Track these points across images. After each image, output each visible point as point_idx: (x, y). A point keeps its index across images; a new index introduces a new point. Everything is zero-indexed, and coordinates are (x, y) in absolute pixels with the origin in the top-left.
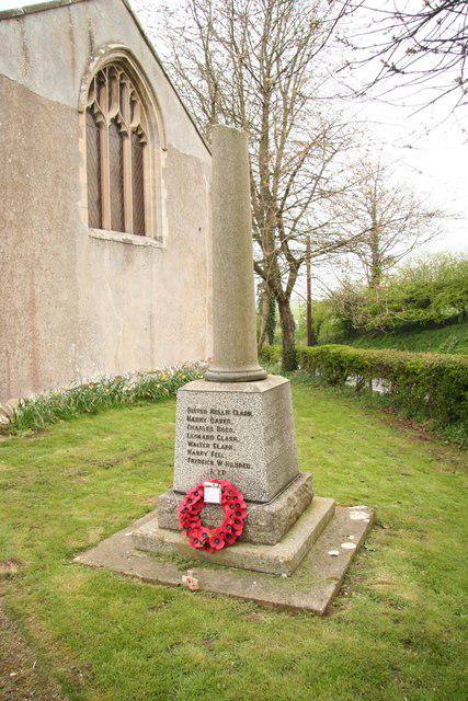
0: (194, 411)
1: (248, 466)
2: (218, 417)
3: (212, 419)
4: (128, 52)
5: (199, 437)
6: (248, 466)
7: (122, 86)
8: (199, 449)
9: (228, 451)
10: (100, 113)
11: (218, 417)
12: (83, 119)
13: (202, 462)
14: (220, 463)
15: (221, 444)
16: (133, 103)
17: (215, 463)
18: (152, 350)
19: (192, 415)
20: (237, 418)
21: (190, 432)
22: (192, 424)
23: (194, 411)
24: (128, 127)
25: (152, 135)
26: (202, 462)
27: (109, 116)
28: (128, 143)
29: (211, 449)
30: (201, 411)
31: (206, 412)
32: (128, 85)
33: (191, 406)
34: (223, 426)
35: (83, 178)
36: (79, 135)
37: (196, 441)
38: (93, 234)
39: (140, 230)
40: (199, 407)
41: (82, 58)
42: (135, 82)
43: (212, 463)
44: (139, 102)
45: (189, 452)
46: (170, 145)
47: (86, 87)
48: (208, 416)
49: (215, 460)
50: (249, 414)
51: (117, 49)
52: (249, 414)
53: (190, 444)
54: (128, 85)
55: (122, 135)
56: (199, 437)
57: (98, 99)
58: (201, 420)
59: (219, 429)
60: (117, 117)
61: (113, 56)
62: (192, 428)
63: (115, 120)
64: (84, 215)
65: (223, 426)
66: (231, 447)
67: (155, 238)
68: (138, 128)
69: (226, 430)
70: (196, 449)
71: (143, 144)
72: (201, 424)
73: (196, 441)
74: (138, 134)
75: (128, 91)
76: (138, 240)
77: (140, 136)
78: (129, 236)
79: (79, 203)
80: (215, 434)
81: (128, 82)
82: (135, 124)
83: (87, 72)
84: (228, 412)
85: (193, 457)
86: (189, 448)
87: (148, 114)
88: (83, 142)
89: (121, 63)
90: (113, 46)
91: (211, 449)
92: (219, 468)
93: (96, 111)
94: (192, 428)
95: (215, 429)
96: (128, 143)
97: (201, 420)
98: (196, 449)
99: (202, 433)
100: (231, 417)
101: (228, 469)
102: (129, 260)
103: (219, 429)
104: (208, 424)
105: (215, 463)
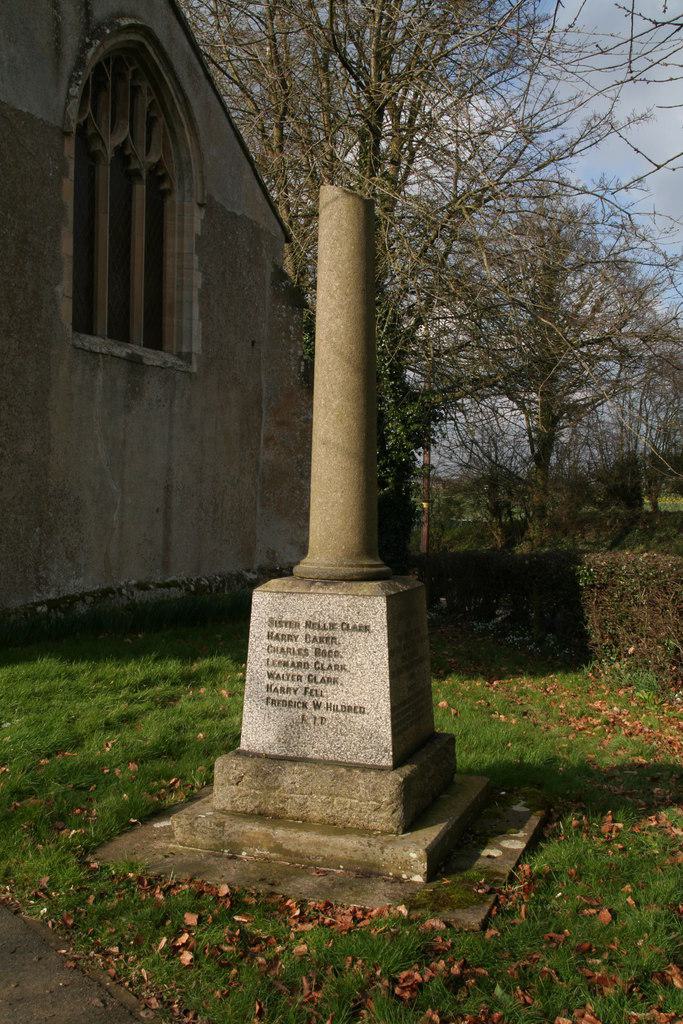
0: (280, 623)
1: (362, 710)
2: (317, 633)
3: (307, 636)
4: (148, 33)
5: (286, 664)
6: (362, 710)
7: (135, 90)
8: (285, 684)
9: (330, 687)
10: (98, 135)
11: (317, 633)
12: (70, 148)
13: (289, 704)
14: (317, 706)
15: (321, 675)
16: (151, 122)
17: (310, 705)
18: (167, 547)
19: (276, 631)
20: (347, 635)
21: (272, 656)
22: (275, 644)
23: (280, 623)
24: (143, 161)
25: (181, 179)
26: (289, 704)
27: (113, 142)
28: (140, 191)
29: (305, 683)
30: (289, 624)
31: (297, 625)
32: (145, 91)
33: (274, 615)
34: (324, 647)
35: (67, 246)
36: (64, 173)
37: (280, 671)
38: (78, 343)
39: (155, 340)
40: (287, 617)
41: (71, 42)
42: (158, 86)
43: (305, 705)
44: (162, 120)
45: (269, 688)
46: (210, 198)
47: (76, 91)
48: (301, 632)
49: (309, 701)
50: (366, 629)
51: (131, 27)
52: (366, 629)
53: (270, 676)
54: (145, 91)
56: (286, 664)
58: (290, 637)
60: (124, 143)
61: (122, 38)
62: (275, 650)
63: (120, 150)
64: (66, 309)
65: (324, 647)
66: (335, 681)
67: (179, 355)
68: (159, 165)
70: (280, 684)
71: (165, 194)
72: (290, 644)
73: (280, 671)
74: (157, 178)
75: (145, 101)
76: (152, 357)
77: (162, 179)
78: (139, 350)
79: (59, 289)
80: (311, 659)
81: (145, 85)
82: (154, 159)
83: (80, 63)
84: (333, 626)
85: (274, 696)
86: (269, 681)
87: (175, 141)
88: (68, 185)
89: (135, 52)
90: (125, 22)
91: (305, 683)
92: (317, 713)
93: (90, 131)
94: (275, 650)
95: (311, 653)
96: (140, 191)
97: (290, 637)
98: (280, 684)
99: (290, 658)
100: (338, 633)
101: (329, 715)
102: (134, 392)
103: (317, 652)
104: (301, 644)
105: (310, 705)
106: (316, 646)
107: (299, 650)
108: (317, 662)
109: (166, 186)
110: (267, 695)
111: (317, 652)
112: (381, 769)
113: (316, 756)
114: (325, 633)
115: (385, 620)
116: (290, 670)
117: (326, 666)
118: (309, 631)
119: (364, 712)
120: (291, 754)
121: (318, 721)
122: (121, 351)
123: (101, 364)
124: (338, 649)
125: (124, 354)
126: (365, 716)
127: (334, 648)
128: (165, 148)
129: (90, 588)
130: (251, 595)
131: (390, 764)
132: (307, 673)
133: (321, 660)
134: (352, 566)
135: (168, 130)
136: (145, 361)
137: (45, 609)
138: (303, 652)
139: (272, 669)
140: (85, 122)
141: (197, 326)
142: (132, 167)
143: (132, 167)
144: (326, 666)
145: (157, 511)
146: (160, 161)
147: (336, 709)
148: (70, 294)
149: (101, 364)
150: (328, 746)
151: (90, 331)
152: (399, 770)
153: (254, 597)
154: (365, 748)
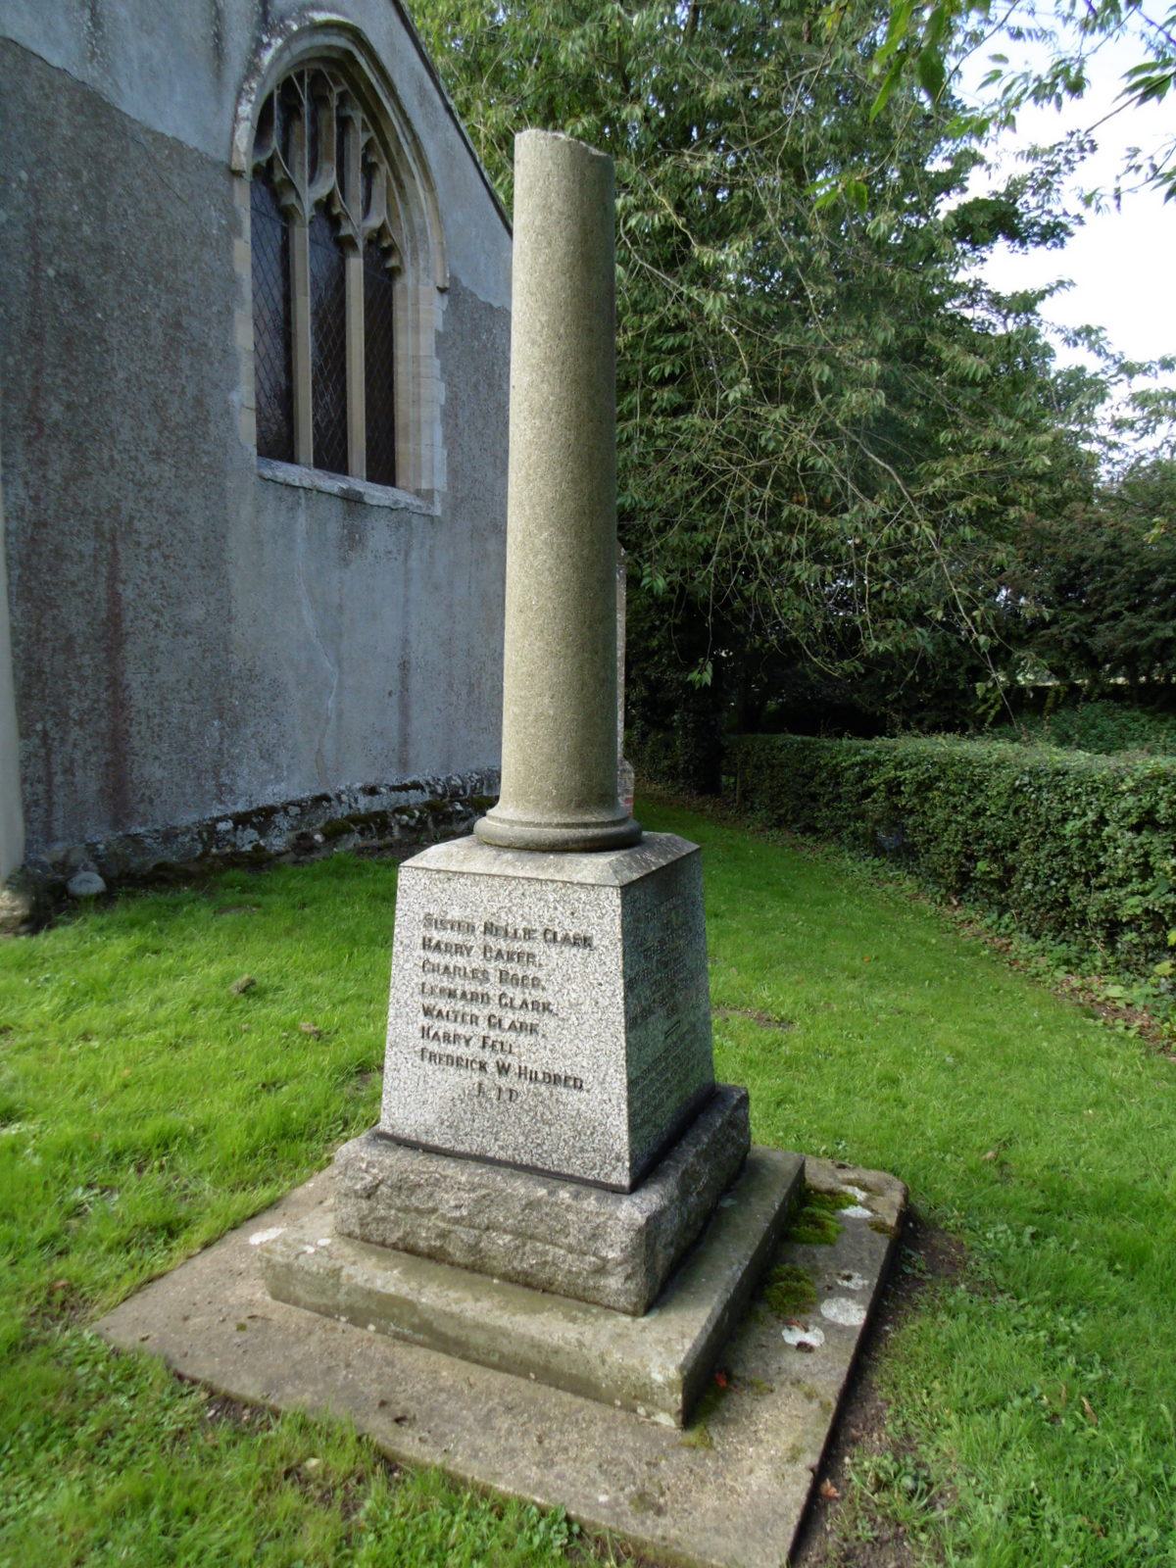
0: (441, 924)
1: (578, 1085)
2: (503, 945)
3: (486, 949)
4: (355, 34)
5: (452, 994)
6: (578, 1085)
7: (344, 123)
8: (451, 1027)
9: (525, 1040)
10: (290, 184)
11: (503, 945)
12: (242, 197)
13: (457, 1062)
14: (503, 1070)
15: (509, 1017)
16: (369, 170)
17: (491, 1068)
18: (405, 741)
19: (436, 936)
20: (554, 951)
21: (431, 979)
22: (435, 958)
23: (441, 924)
24: (359, 225)
25: (415, 251)
26: (457, 1062)
27: (310, 194)
28: (356, 266)
30: (457, 926)
31: (471, 928)
32: (358, 124)
33: (435, 910)
34: (515, 968)
35: (244, 336)
36: (233, 229)
37: (443, 1005)
38: (268, 473)
39: (383, 469)
40: (455, 914)
41: (238, 39)
42: (375, 117)
43: (483, 1067)
44: (384, 167)
46: (454, 279)
47: (247, 109)
48: (476, 940)
49: (491, 1059)
50: (586, 942)
51: (328, 26)
52: (586, 942)
53: (427, 1012)
54: (358, 124)
55: (345, 245)
56: (452, 994)
57: (285, 148)
58: (459, 949)
59: (503, 977)
60: (331, 196)
61: (322, 40)
62: (435, 969)
63: (325, 206)
64: (247, 427)
65: (515, 968)
66: (533, 1029)
67: (418, 493)
68: (382, 232)
69: (520, 982)
70: (442, 1027)
71: (393, 273)
72: (459, 961)
73: (443, 1005)
74: (382, 254)
75: (359, 138)
76: (376, 494)
77: (389, 252)
78: (358, 483)
79: (235, 397)
80: (493, 989)
81: (358, 116)
82: (375, 222)
83: (252, 69)
84: (529, 934)
85: (434, 1047)
87: (405, 202)
88: (242, 250)
89: (343, 63)
90: (320, 17)
91: (482, 1029)
92: (504, 1082)
93: (278, 176)
94: (435, 969)
95: (494, 977)
96: (356, 266)
97: (459, 949)
98: (442, 1027)
99: (459, 984)
100: (537, 947)
101: (523, 1086)
102: (353, 540)
103: (503, 977)
104: (476, 961)
105: (491, 1068)
106: (501, 966)
108: (503, 995)
109: (393, 262)
110: (421, 1043)
113: (502, 1155)
114: (516, 946)
115: (618, 930)
116: (459, 1005)
117: (518, 1002)
118: (491, 940)
120: (460, 1148)
121: (505, 1096)
122: (334, 484)
123: (303, 501)
124: (540, 975)
125: (335, 490)
126: (584, 1094)
127: (532, 971)
128: (390, 208)
129: (297, 794)
131: (626, 1182)
132: (486, 1012)
135: (394, 184)
136: (366, 499)
137: (229, 825)
139: (430, 1001)
140: (270, 162)
141: (440, 454)
142: (343, 233)
143: (343, 233)
145: (390, 694)
146: (383, 226)
147: (534, 1079)
148: (253, 404)
149: (303, 501)
150: (521, 1139)
151: (290, 457)
154: (582, 1150)
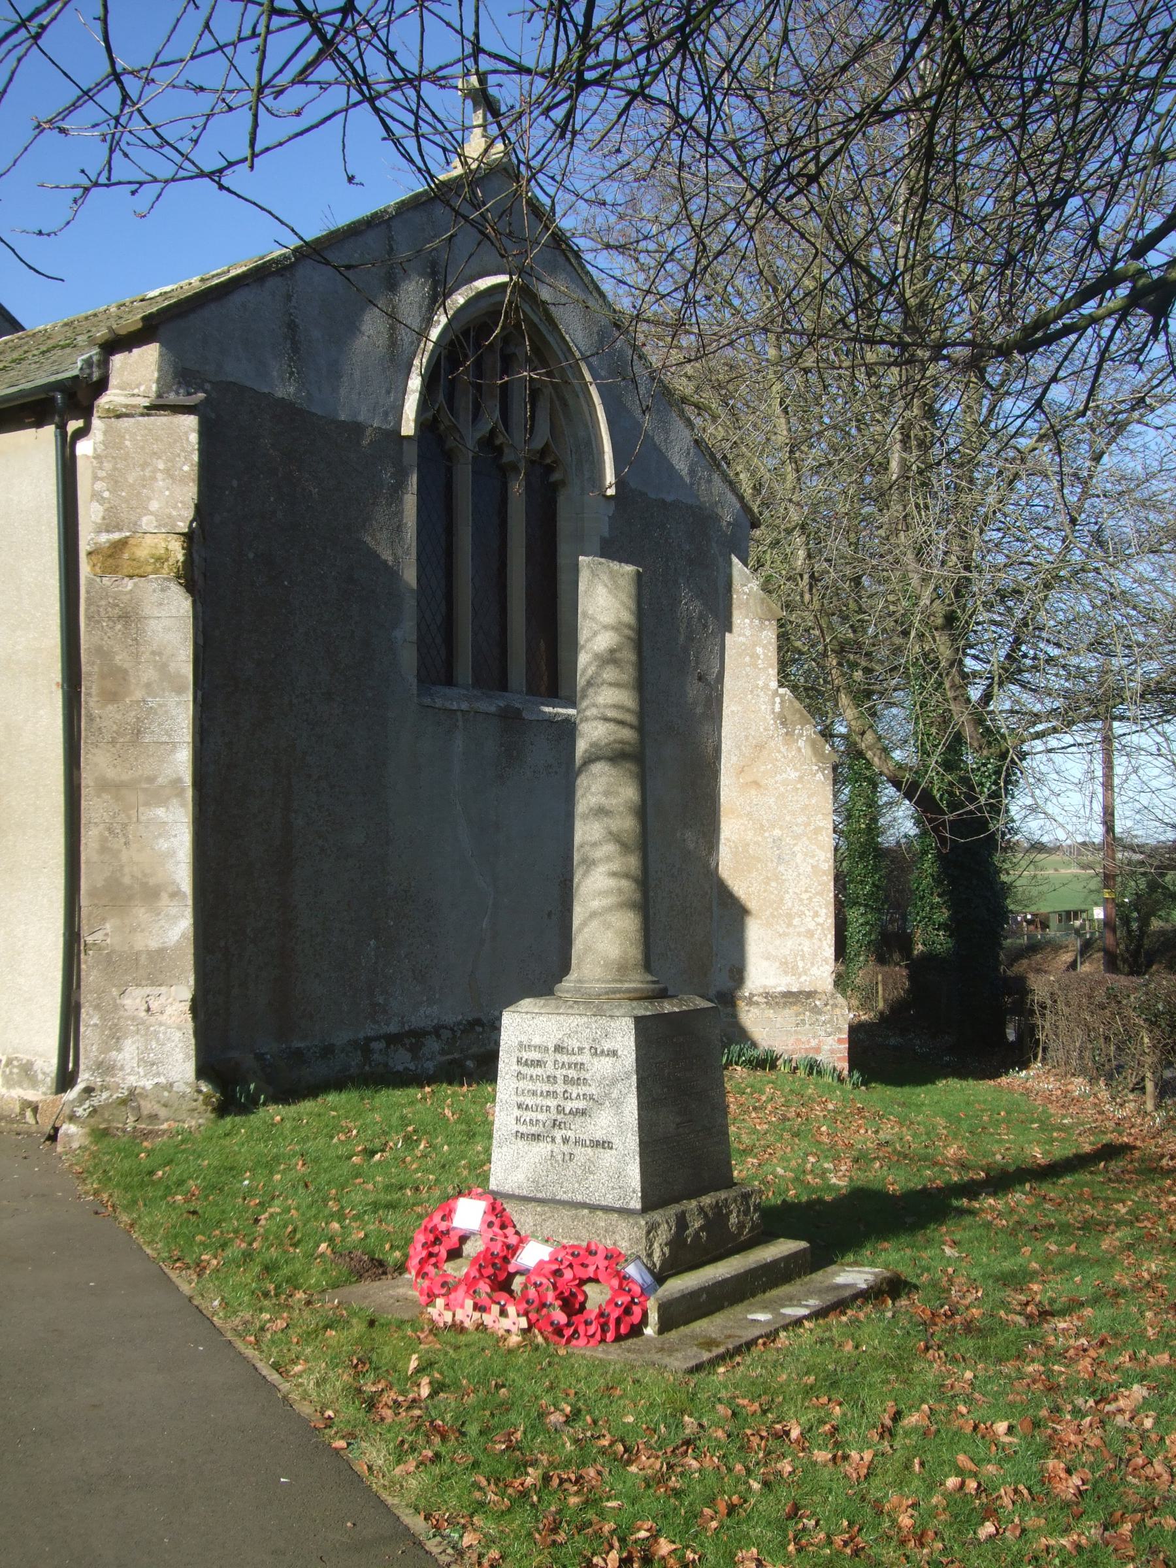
5: (534, 1093)
19: (525, 1055)
20: (596, 1060)
21: (522, 1084)
29: (553, 1115)
31: (547, 1049)
33: (524, 1039)
40: (536, 1040)
45: (518, 1120)
50: (614, 1053)
52: (614, 1053)
53: (519, 1106)
56: (534, 1093)
58: (538, 1063)
59: (566, 1080)
65: (572, 1073)
69: (577, 1082)
72: (539, 1071)
73: (529, 1101)
84: (581, 1049)
92: (565, 1149)
95: (560, 1080)
97: (538, 1063)
98: (528, 1116)
101: (578, 1150)
104: (550, 1069)
105: (559, 1140)
106: (564, 1072)
107: (548, 1077)
108: (566, 1091)
110: (515, 1128)
111: (566, 1080)
112: (624, 1212)
113: (565, 1197)
114: (573, 1059)
115: (633, 1044)
116: (539, 1101)
117: (574, 1095)
118: (559, 1057)
119: (612, 1148)
120: (539, 1195)
121: (567, 1158)
124: (587, 1076)
126: (614, 1152)
127: (583, 1075)
130: (499, 1018)
131: (638, 1206)
132: (555, 1103)
133: (570, 1088)
134: (608, 982)
138: (551, 1079)
139: (521, 1099)
144: (574, 1095)
147: (584, 1145)
150: (576, 1185)
152: (647, 1217)
153: (504, 1018)
154: (613, 1188)
